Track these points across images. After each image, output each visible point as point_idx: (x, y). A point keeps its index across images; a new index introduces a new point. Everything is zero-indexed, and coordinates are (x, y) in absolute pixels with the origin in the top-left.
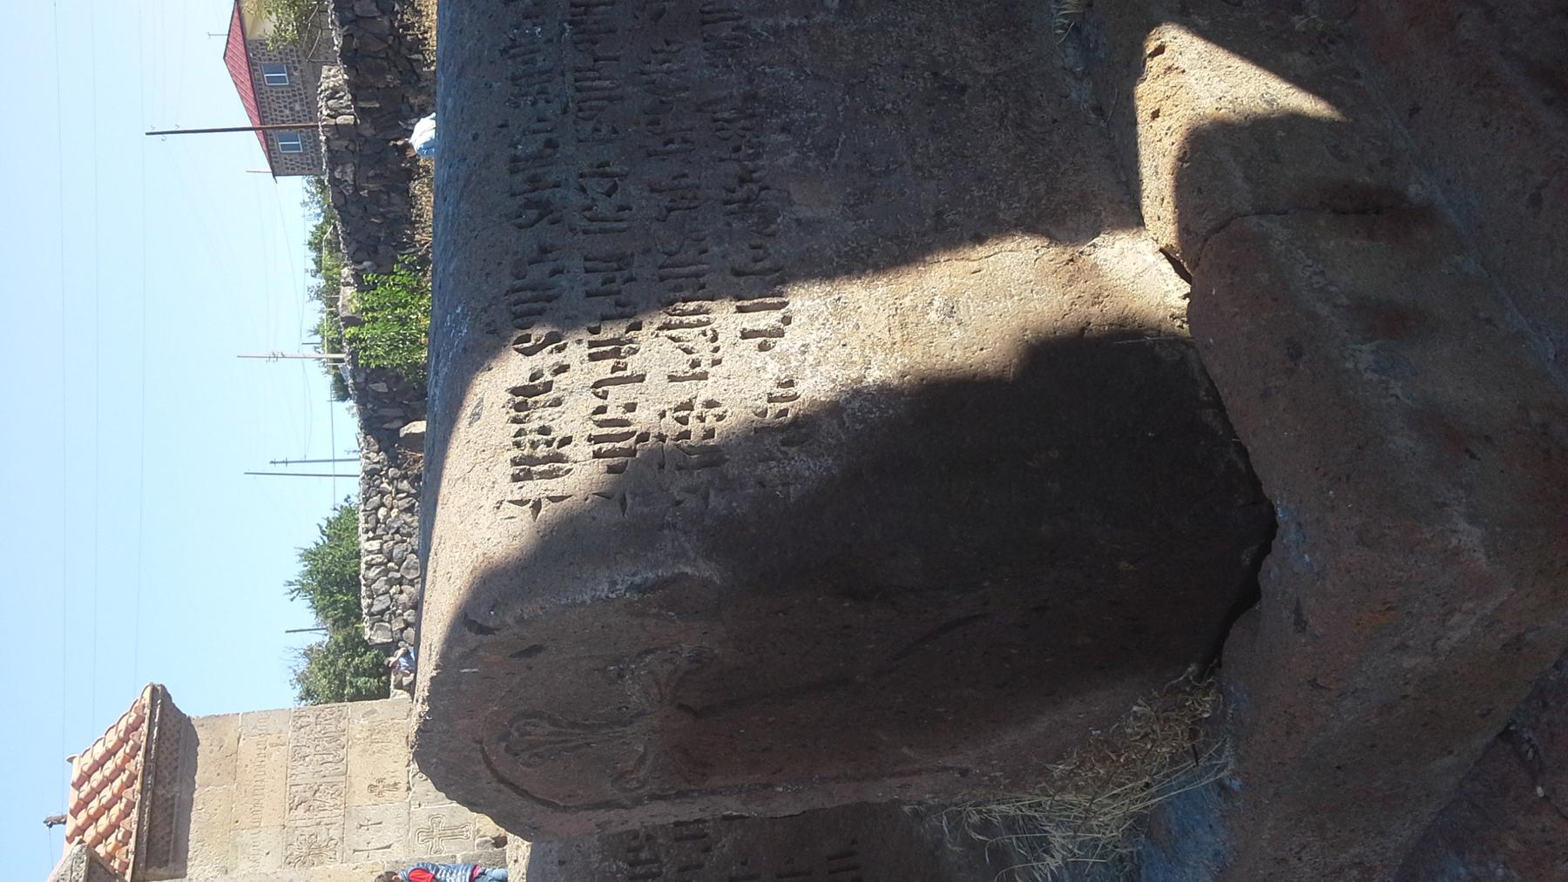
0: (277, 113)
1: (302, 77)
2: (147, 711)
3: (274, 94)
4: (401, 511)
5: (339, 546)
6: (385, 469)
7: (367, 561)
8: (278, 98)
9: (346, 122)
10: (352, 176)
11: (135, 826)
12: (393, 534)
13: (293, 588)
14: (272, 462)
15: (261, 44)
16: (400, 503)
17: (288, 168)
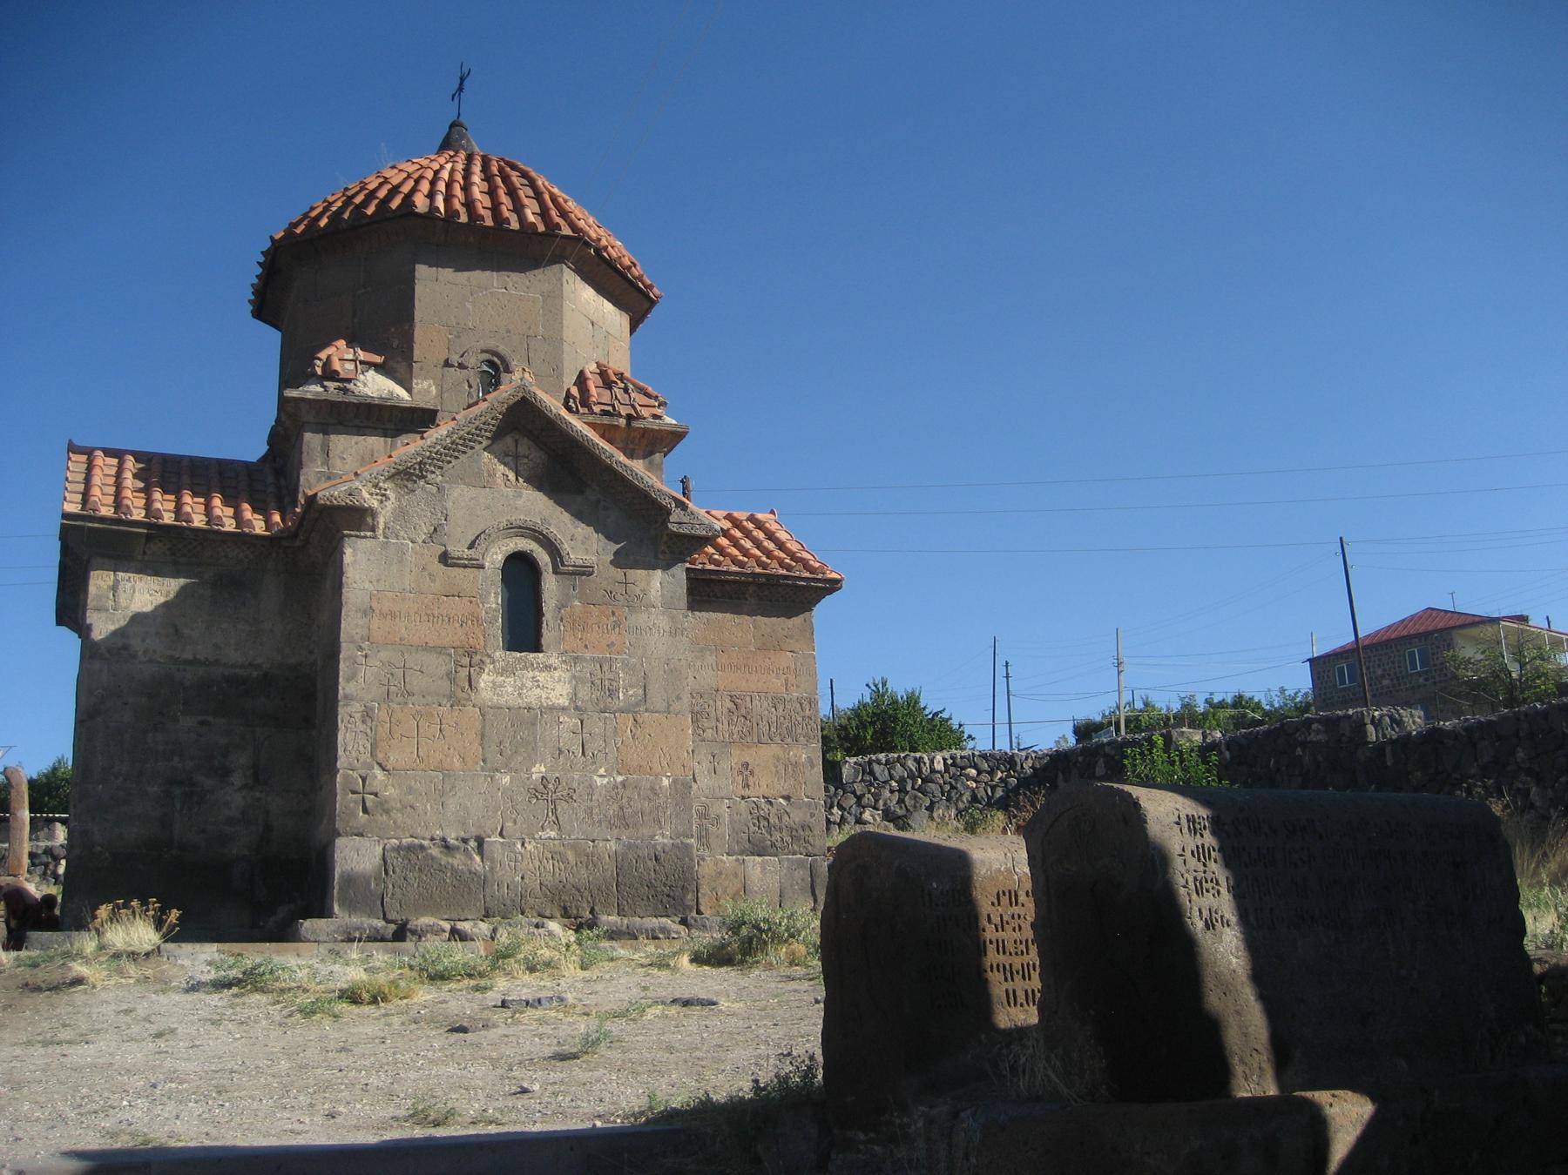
0: (1377, 662)
1: (1419, 686)
2: (820, 576)
3: (1397, 658)
4: (973, 790)
5: (923, 731)
6: (1016, 774)
7: (923, 758)
8: (1393, 663)
9: (1369, 734)
10: (1315, 739)
11: (725, 569)
12: (950, 783)
13: (880, 686)
14: (1007, 663)
15: (1449, 645)
16: (982, 790)
17: (1319, 673)
